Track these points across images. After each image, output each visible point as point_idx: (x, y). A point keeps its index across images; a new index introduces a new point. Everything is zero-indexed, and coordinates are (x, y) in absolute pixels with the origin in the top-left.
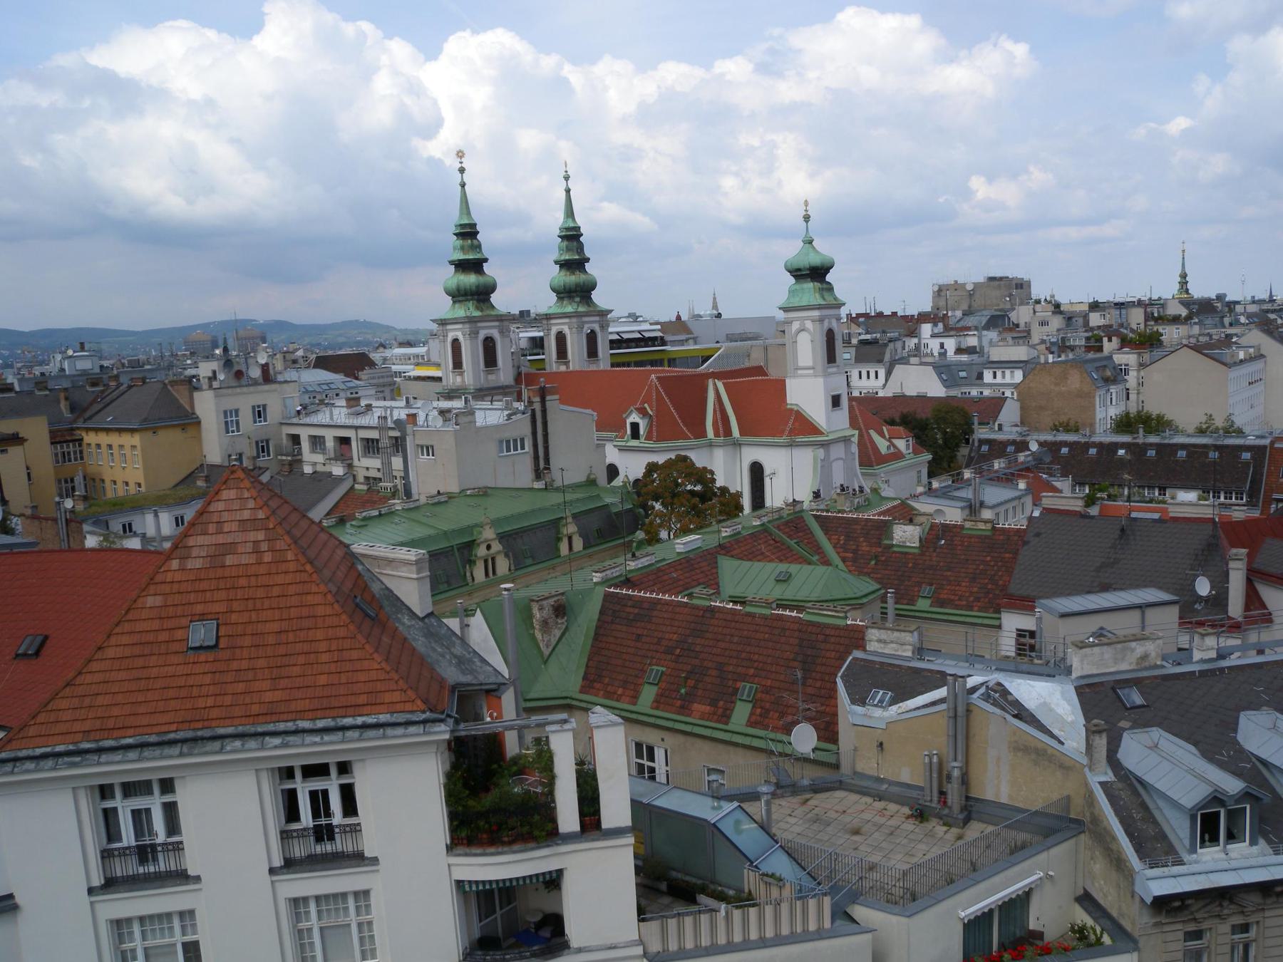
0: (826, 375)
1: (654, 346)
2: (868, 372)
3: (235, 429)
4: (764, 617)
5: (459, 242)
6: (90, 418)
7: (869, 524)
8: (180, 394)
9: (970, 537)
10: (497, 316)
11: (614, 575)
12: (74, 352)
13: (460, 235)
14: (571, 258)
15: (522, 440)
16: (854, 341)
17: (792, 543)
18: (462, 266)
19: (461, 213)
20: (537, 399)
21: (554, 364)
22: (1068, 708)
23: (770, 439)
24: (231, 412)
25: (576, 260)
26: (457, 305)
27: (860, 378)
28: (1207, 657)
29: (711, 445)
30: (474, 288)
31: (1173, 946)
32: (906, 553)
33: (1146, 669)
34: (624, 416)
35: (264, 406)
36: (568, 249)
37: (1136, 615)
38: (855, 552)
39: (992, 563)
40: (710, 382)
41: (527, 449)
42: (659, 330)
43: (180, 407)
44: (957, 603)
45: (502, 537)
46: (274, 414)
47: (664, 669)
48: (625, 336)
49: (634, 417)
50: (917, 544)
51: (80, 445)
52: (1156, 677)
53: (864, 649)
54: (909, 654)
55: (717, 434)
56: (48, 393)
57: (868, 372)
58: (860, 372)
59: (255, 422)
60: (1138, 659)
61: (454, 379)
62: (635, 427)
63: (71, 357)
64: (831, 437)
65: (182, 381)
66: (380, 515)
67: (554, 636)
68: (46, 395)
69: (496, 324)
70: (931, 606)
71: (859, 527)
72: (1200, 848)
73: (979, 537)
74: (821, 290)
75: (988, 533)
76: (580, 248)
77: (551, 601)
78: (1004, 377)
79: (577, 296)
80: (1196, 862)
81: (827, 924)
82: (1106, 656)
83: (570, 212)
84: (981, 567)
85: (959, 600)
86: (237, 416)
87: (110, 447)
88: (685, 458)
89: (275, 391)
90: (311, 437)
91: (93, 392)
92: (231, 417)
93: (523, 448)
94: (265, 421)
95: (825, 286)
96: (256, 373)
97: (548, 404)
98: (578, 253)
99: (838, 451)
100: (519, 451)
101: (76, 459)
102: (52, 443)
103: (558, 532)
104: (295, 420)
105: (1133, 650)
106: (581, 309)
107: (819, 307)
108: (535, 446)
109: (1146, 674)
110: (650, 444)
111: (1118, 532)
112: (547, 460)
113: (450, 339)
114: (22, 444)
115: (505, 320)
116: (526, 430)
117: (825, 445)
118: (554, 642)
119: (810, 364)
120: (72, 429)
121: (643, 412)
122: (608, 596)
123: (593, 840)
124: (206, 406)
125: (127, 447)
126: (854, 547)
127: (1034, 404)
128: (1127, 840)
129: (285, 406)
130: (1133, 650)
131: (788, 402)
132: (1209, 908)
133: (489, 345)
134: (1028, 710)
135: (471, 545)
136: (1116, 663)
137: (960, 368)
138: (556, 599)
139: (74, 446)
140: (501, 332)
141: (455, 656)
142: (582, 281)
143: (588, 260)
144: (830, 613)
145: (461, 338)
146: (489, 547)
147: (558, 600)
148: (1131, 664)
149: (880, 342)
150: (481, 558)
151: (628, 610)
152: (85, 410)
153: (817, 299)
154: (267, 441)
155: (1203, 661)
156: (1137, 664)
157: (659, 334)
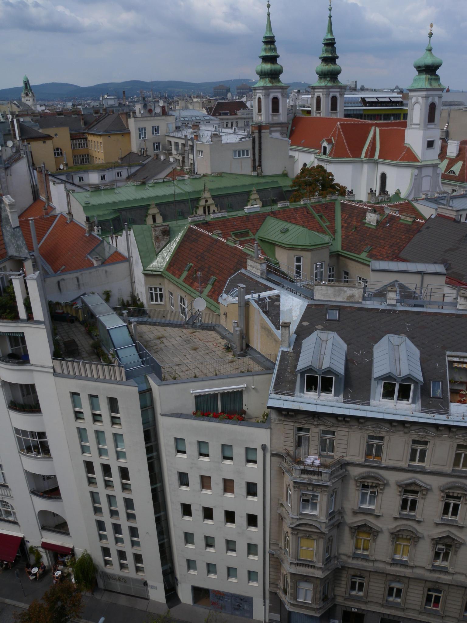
0: (425, 128)
1: (397, 106)
3: (144, 137)
4: (231, 247)
5: (264, 46)
6: (90, 129)
7: (362, 210)
8: (123, 118)
9: (402, 224)
10: (280, 86)
11: (199, 219)
12: (108, 96)
13: (266, 43)
14: (327, 56)
15: (247, 151)
17: (316, 215)
18: (265, 59)
19: (267, 30)
20: (257, 131)
21: (315, 113)
22: (298, 313)
23: (390, 162)
24: (142, 129)
25: (329, 57)
26: (261, 80)
28: (390, 303)
29: (362, 162)
30: (269, 71)
31: (288, 431)
32: (370, 228)
33: (352, 302)
34: (321, 142)
35: (158, 127)
36: (327, 51)
37: (418, 278)
39: (404, 240)
40: (373, 128)
41: (249, 156)
42: (401, 97)
43: (123, 125)
44: (378, 257)
45: (214, 197)
46: (163, 130)
47: (192, 265)
48: (380, 100)
49: (325, 144)
50: (375, 224)
51: (86, 141)
52: (355, 308)
53: (246, 270)
54: (259, 274)
55: (366, 157)
56: (77, 116)
59: (153, 134)
60: (348, 297)
61: (258, 118)
62: (325, 148)
63: (106, 98)
64: (423, 163)
65: (124, 113)
66: (164, 182)
67: (162, 244)
68: (76, 117)
69: (280, 90)
70: (366, 257)
72: (307, 390)
73: (405, 225)
75: (410, 223)
76: (334, 50)
77: (161, 228)
79: (328, 77)
80: (301, 397)
81: (124, 379)
82: (329, 292)
83: (330, 30)
85: (380, 256)
86: (145, 131)
87: (94, 141)
88: (322, 167)
89: (164, 119)
90: (175, 142)
91: (96, 116)
92: (142, 131)
93: (247, 155)
94: (158, 133)
96: (158, 110)
97: (263, 134)
98: (331, 53)
99: (428, 171)
100: (245, 156)
101: (84, 147)
102: (71, 139)
103: (249, 198)
104: (172, 134)
105: (345, 292)
106: (330, 84)
107: (426, 90)
108: (254, 154)
109: (351, 305)
110: (329, 158)
112: (260, 161)
113: (257, 98)
114: (51, 139)
116: (249, 146)
117: (420, 168)
118: (161, 246)
119: (418, 122)
120: (85, 133)
121: (329, 142)
122: (190, 229)
123: (31, 324)
124: (132, 124)
125: (99, 143)
126: (349, 221)
128: (275, 379)
129: (168, 127)
130: (345, 292)
131: (405, 142)
132: (307, 419)
133: (275, 101)
134: (280, 310)
135: (198, 199)
136: (335, 297)
138: (163, 227)
139: (84, 141)
140: (282, 95)
141: (17, 245)
142: (331, 69)
143: (337, 57)
144: (251, 250)
145: (261, 97)
146: (206, 201)
147: (165, 228)
148: (343, 298)
150: (201, 206)
151: (193, 236)
152: (91, 124)
153: (426, 85)
154: (159, 143)
155: (388, 305)
156: (347, 299)
157: (400, 100)
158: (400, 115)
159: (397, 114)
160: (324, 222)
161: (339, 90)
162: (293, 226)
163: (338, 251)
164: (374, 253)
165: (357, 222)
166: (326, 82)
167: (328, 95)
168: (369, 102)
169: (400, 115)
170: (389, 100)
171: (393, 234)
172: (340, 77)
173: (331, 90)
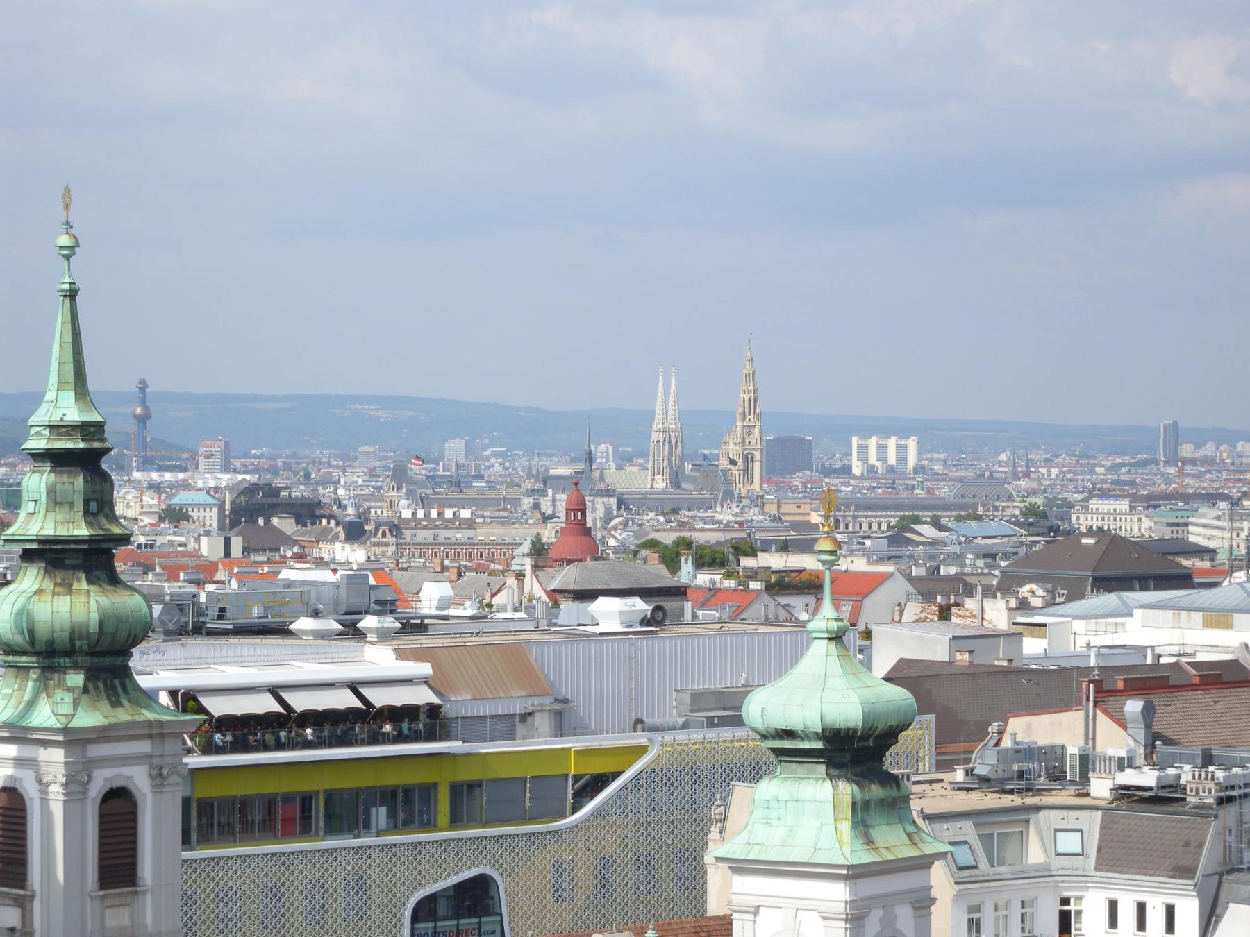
2: (1141, 908)
16: (1101, 787)
27: (1113, 922)
36: (55, 500)
42: (425, 681)
48: (301, 702)
57: (1141, 908)
58: (1113, 905)
74: (862, 816)
79: (76, 667)
95: (876, 791)
98: (90, 516)
106: (90, 718)
149: (1192, 800)
157: (422, 696)
158: (429, 790)
159: (408, 792)
161: (144, 747)
166: (65, 701)
168: (226, 723)
169: (429, 790)
170: (352, 702)
173: (96, 751)
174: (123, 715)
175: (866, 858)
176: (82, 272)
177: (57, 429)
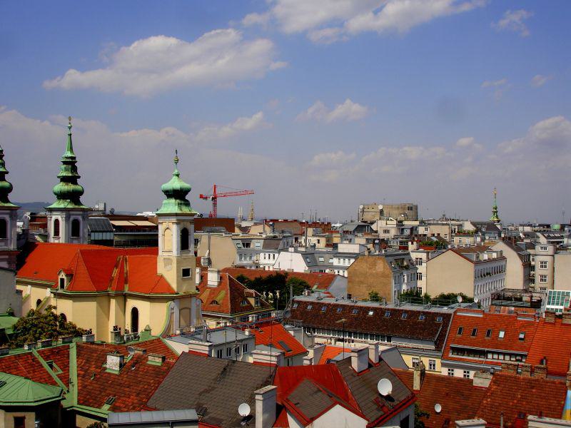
9: (150, 366)
36: (66, 170)
38: (86, 371)
71: (95, 355)
76: (74, 169)
78: (344, 262)
84: (146, 387)
111: (222, 370)
115: (87, 212)
127: (357, 280)
137: (321, 255)
160: (56, 371)
161: (81, 213)
162: (13, 377)
163: (73, 407)
164: (117, 404)
165: (96, 368)
166: (66, 204)
167: (67, 218)
171: (139, 379)
172: (82, 199)
173: (71, 213)
174: (77, 207)
175: (180, 212)
176: (72, 131)
177: (66, 158)
